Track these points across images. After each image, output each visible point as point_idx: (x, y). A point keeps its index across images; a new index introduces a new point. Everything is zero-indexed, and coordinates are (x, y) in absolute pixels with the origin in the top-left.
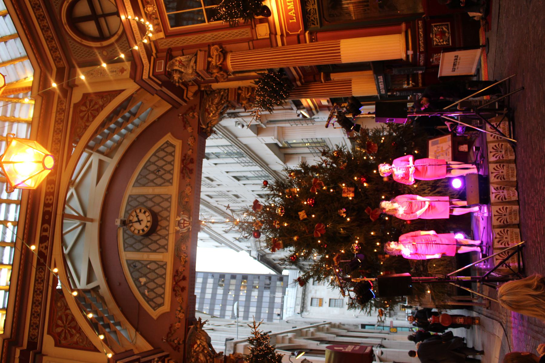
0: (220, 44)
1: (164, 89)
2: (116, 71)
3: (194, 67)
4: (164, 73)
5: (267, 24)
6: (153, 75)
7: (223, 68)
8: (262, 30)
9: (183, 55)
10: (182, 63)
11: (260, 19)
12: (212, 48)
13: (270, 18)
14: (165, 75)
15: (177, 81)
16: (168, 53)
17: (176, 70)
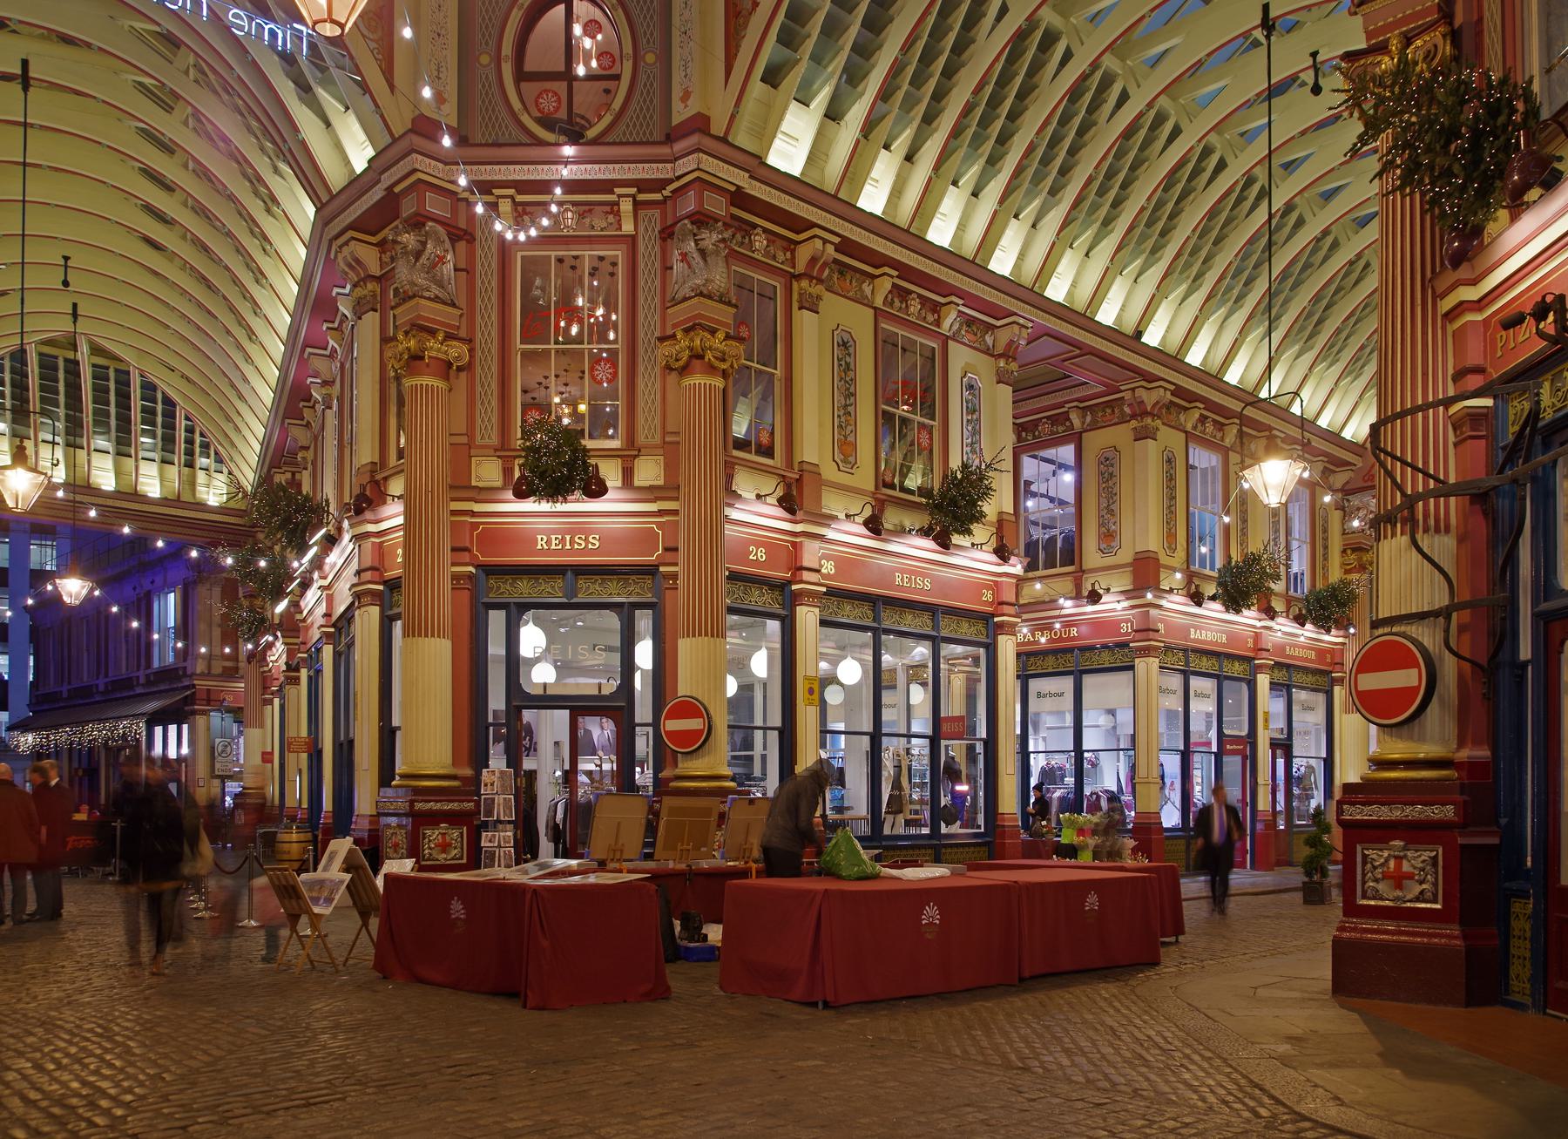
0: (469, 367)
1: (377, 194)
2: (439, 78)
3: (426, 294)
4: (422, 212)
5: (499, 484)
6: (420, 180)
7: (415, 359)
8: (488, 471)
9: (455, 270)
10: (436, 265)
11: (512, 470)
12: (465, 348)
13: (509, 495)
14: (417, 214)
15: (399, 239)
16: (466, 232)
17: (424, 244)
